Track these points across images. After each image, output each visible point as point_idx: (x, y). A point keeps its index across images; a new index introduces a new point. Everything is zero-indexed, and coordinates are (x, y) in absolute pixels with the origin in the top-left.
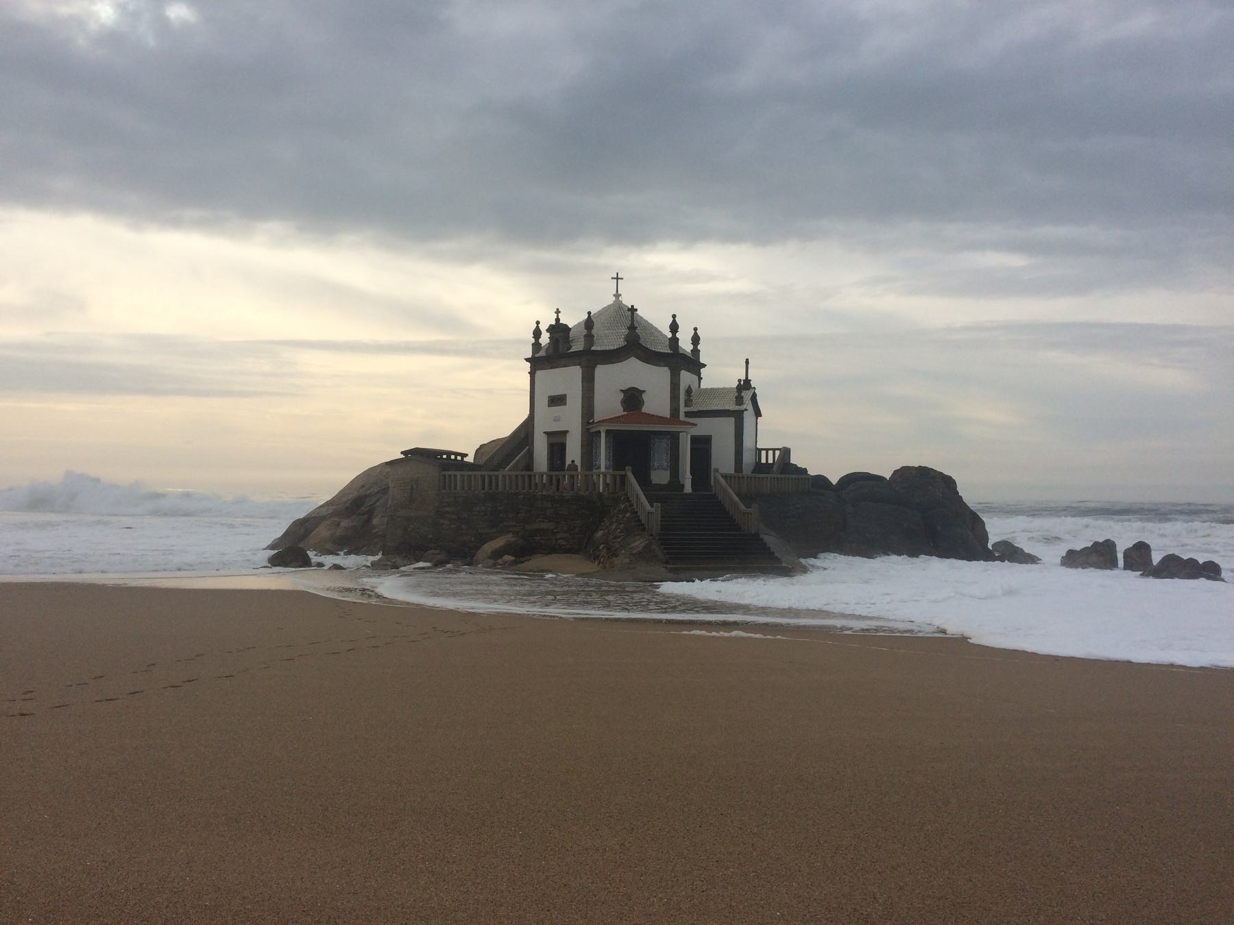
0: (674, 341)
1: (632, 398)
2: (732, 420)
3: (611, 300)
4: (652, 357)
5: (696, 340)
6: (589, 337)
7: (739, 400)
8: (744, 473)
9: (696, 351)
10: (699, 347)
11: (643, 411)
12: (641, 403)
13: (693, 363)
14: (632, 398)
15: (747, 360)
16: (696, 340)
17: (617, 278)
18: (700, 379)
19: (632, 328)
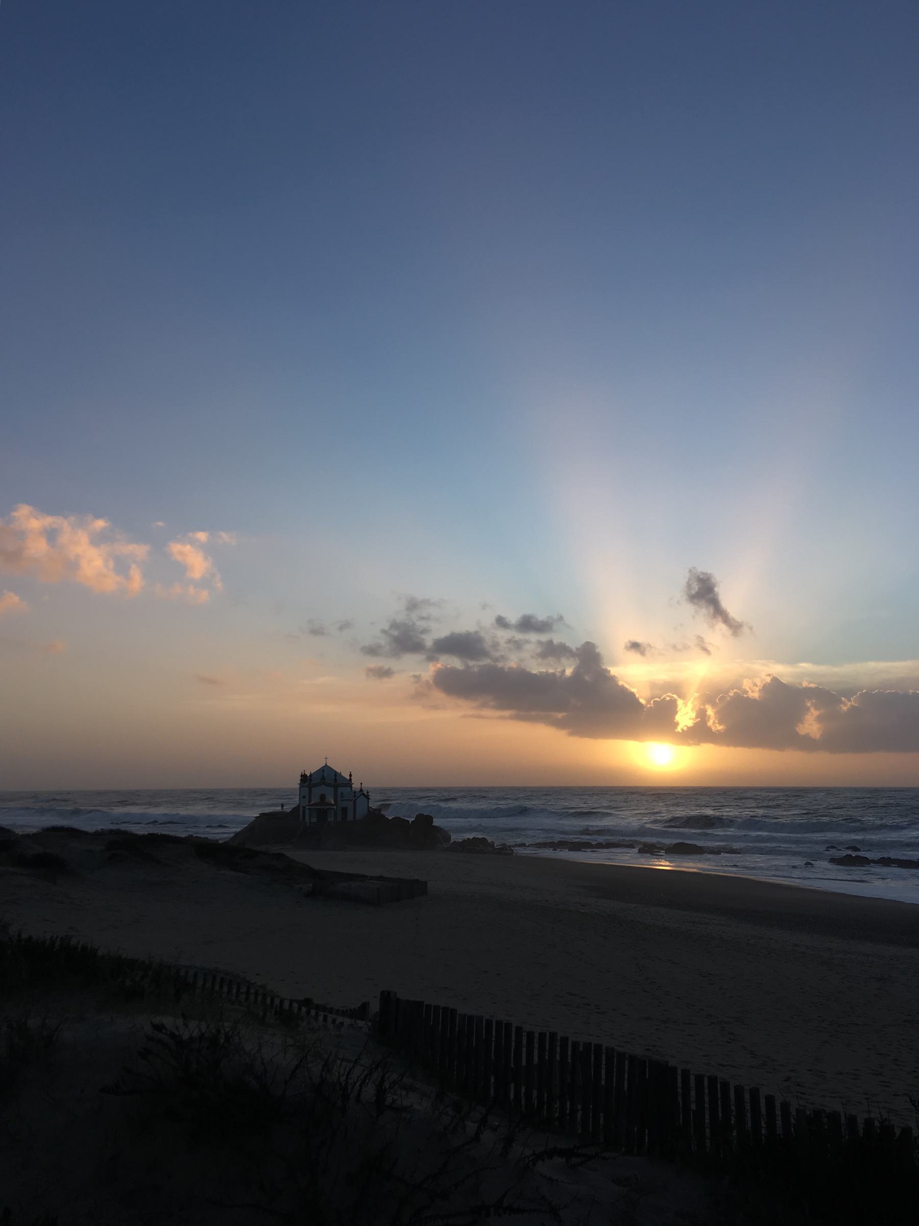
0: (335, 779)
1: (323, 797)
2: (352, 803)
3: (324, 765)
4: (329, 785)
5: (351, 775)
6: (311, 780)
7: (355, 796)
8: (356, 819)
9: (350, 780)
10: (352, 778)
11: (326, 801)
12: (325, 798)
13: (349, 783)
14: (323, 797)
15: (361, 784)
16: (351, 775)
17: (326, 758)
18: (351, 788)
19: (323, 776)
